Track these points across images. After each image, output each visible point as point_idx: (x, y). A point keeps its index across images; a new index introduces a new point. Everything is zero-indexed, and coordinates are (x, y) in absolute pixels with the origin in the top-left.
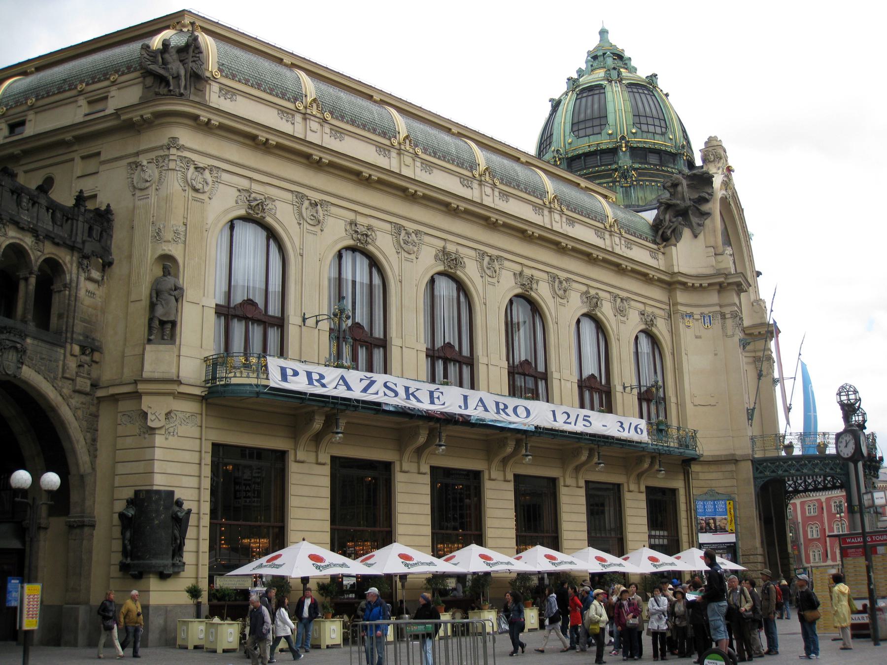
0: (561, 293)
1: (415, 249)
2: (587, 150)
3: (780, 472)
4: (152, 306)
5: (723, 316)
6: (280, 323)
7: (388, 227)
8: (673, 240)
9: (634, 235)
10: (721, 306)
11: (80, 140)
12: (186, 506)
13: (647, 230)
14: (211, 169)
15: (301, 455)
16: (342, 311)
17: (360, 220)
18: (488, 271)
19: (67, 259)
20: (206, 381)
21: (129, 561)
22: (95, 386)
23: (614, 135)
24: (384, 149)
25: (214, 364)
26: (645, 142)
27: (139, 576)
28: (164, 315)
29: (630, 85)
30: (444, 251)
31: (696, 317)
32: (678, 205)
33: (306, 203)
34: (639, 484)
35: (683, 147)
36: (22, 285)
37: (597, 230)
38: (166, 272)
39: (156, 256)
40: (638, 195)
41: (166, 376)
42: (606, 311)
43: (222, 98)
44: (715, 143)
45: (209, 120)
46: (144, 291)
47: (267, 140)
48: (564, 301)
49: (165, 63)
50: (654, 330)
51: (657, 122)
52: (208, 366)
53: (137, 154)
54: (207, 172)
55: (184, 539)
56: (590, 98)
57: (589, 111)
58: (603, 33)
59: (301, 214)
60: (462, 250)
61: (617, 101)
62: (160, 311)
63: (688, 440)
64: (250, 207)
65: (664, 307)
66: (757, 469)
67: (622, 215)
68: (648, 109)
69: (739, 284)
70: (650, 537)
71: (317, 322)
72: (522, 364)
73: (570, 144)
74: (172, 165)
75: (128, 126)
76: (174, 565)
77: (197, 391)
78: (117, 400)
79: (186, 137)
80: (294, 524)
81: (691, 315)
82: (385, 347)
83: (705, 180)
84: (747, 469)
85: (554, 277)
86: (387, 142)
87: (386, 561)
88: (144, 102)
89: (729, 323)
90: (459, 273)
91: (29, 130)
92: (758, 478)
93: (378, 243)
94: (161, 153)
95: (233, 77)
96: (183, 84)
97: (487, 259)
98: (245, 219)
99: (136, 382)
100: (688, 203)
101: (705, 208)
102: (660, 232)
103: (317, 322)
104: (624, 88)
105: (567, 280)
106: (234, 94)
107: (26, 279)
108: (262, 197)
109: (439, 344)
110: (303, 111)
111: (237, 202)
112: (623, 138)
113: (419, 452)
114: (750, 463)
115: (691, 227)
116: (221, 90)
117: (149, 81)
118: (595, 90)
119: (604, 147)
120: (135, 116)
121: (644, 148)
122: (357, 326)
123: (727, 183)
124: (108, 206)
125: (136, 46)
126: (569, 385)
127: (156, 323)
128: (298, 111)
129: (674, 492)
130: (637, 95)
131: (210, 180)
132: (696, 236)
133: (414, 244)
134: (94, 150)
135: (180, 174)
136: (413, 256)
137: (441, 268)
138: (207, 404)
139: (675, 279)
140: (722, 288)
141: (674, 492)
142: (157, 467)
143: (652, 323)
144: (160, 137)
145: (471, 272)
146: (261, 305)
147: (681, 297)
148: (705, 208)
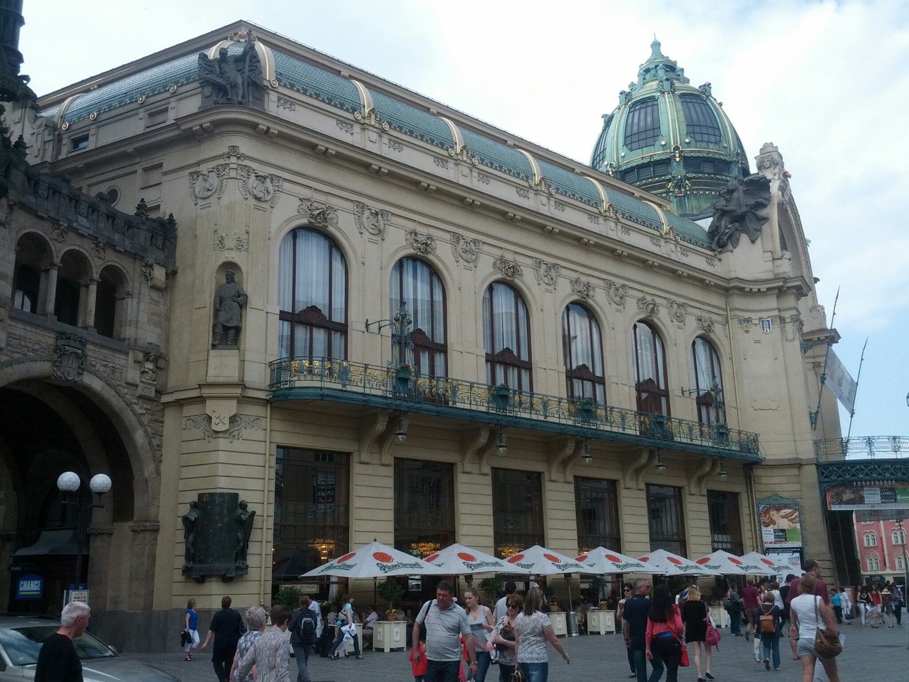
0: (617, 299)
1: (474, 257)
2: (639, 163)
3: (848, 477)
4: (217, 312)
5: (782, 320)
6: (343, 329)
7: (447, 236)
8: (730, 247)
9: (690, 241)
10: (779, 310)
11: (143, 152)
12: (250, 508)
13: (703, 237)
14: (273, 177)
15: (365, 457)
16: (404, 317)
17: (420, 229)
18: (546, 280)
20: (271, 386)
21: (191, 565)
22: (159, 393)
23: (668, 146)
24: (442, 160)
25: (278, 369)
26: (698, 152)
27: (201, 580)
28: (228, 321)
29: (683, 95)
30: (503, 260)
31: (754, 322)
32: (734, 211)
33: (367, 213)
34: (700, 487)
35: (738, 154)
36: (83, 291)
38: (230, 279)
39: (219, 263)
40: (691, 205)
41: (230, 380)
42: (663, 317)
43: (281, 107)
44: (770, 149)
45: (268, 128)
46: (207, 298)
47: (327, 149)
48: (621, 307)
49: (222, 74)
50: (712, 336)
51: (711, 131)
52: (272, 371)
53: (198, 164)
54: (268, 180)
55: (247, 541)
56: (643, 111)
57: (642, 124)
58: (656, 45)
59: (361, 225)
60: (520, 259)
61: (670, 115)
62: (223, 317)
63: (751, 443)
64: (312, 216)
65: (721, 312)
66: (823, 474)
67: (677, 224)
69: (798, 288)
70: (713, 542)
71: (380, 328)
72: (579, 368)
73: (623, 157)
74: (233, 174)
75: (189, 137)
76: (237, 568)
77: (262, 395)
78: (182, 405)
79: (245, 145)
80: (358, 525)
81: (748, 320)
82: (446, 353)
83: (762, 185)
84: (811, 472)
85: (610, 284)
86: (445, 153)
87: (448, 562)
88: (203, 111)
90: (517, 281)
91: (90, 145)
92: (824, 482)
93: (438, 252)
94: (221, 162)
95: (292, 87)
96: (240, 93)
97: (543, 267)
99: (200, 386)
100: (744, 209)
101: (762, 213)
102: (716, 239)
103: (380, 328)
104: (678, 99)
105: (623, 286)
106: (292, 104)
107: (87, 286)
109: (498, 349)
110: (362, 121)
111: (299, 212)
112: (677, 148)
113: (481, 453)
114: (814, 467)
115: (748, 233)
117: (208, 90)
118: (648, 102)
119: (656, 158)
120: (195, 125)
121: (698, 157)
122: (419, 332)
123: (784, 188)
124: (171, 215)
125: (194, 58)
126: (627, 388)
127: (220, 330)
128: (357, 121)
129: (735, 495)
130: (690, 105)
131: (271, 189)
132: (753, 242)
134: (156, 162)
135: (241, 183)
136: (472, 265)
137: (499, 276)
138: (271, 407)
139: (732, 285)
140: (781, 292)
141: (735, 495)
142: (221, 470)
143: (709, 329)
144: (220, 146)
145: (528, 280)
146: (326, 312)
147: (738, 302)
148: (762, 213)
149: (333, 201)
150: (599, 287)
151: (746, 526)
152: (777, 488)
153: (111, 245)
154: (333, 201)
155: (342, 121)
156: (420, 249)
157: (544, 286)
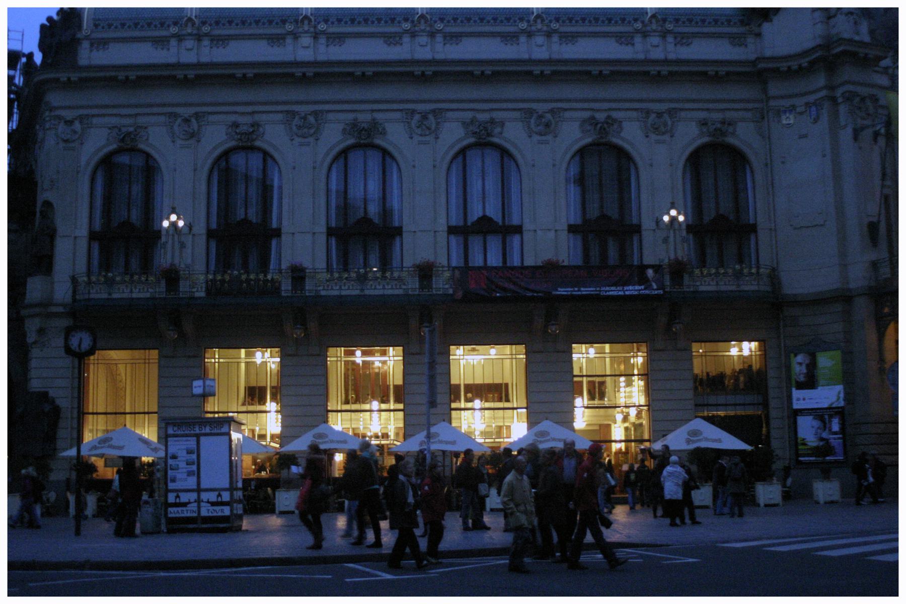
0: (541, 128)
1: (312, 131)
5: (833, 100)
14: (81, 118)
18: (419, 131)
30: (354, 125)
31: (798, 110)
60: (379, 116)
65: (751, 106)
77: (61, 309)
89: (843, 109)
97: (417, 117)
105: (552, 111)
106: (105, 43)
108: (131, 129)
111: (108, 140)
116: (92, 45)
126: (552, 234)
136: (311, 140)
147: (774, 88)
149: (141, 120)
154: (141, 120)
156: (241, 140)
157: (417, 138)
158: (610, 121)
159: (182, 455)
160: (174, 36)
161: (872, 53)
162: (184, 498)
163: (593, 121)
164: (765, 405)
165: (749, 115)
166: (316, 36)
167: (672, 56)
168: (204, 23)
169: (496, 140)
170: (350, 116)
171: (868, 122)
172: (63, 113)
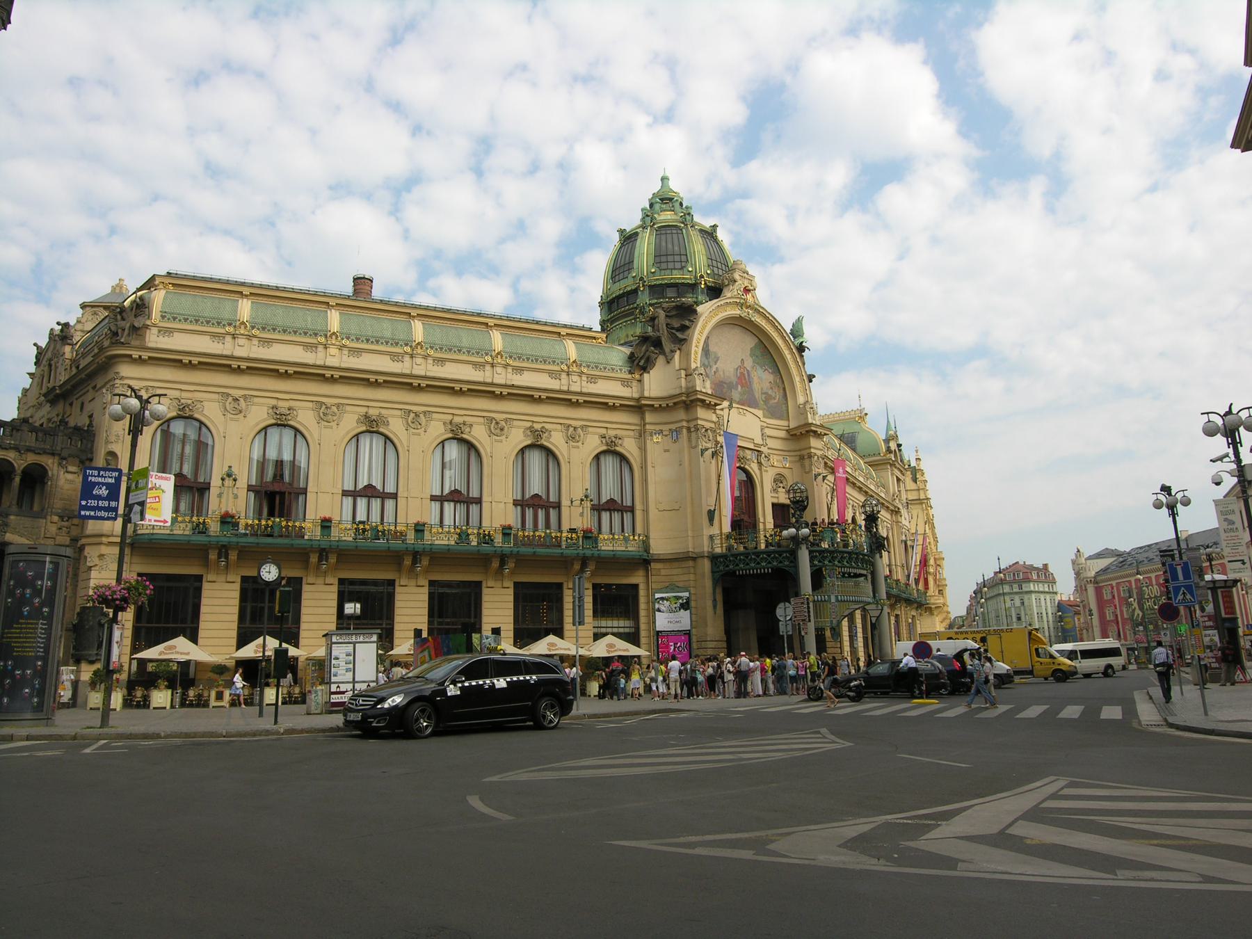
10: (688, 421)
17: (281, 404)
19: (50, 462)
30: (366, 416)
37: (551, 374)
51: (677, 258)
60: (384, 412)
68: (670, 246)
72: (452, 492)
79: (126, 370)
97: (412, 415)
98: (179, 417)
105: (506, 420)
126: (502, 505)
129: (636, 586)
133: (334, 414)
136: (333, 424)
141: (636, 586)
150: (478, 424)
151: (642, 613)
152: (675, 578)
153: (29, 450)
155: (214, 336)
158: (543, 430)
159: (342, 656)
160: (228, 334)
161: (713, 401)
162: (343, 688)
163: (532, 430)
164: (637, 628)
165: (631, 433)
166: (342, 347)
167: (584, 390)
168: (253, 328)
169: (464, 436)
170: (364, 410)
171: (709, 445)
172: (132, 383)
